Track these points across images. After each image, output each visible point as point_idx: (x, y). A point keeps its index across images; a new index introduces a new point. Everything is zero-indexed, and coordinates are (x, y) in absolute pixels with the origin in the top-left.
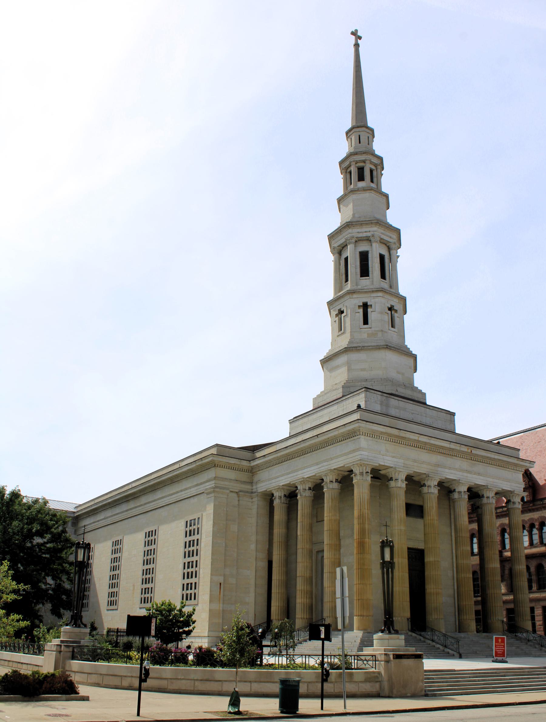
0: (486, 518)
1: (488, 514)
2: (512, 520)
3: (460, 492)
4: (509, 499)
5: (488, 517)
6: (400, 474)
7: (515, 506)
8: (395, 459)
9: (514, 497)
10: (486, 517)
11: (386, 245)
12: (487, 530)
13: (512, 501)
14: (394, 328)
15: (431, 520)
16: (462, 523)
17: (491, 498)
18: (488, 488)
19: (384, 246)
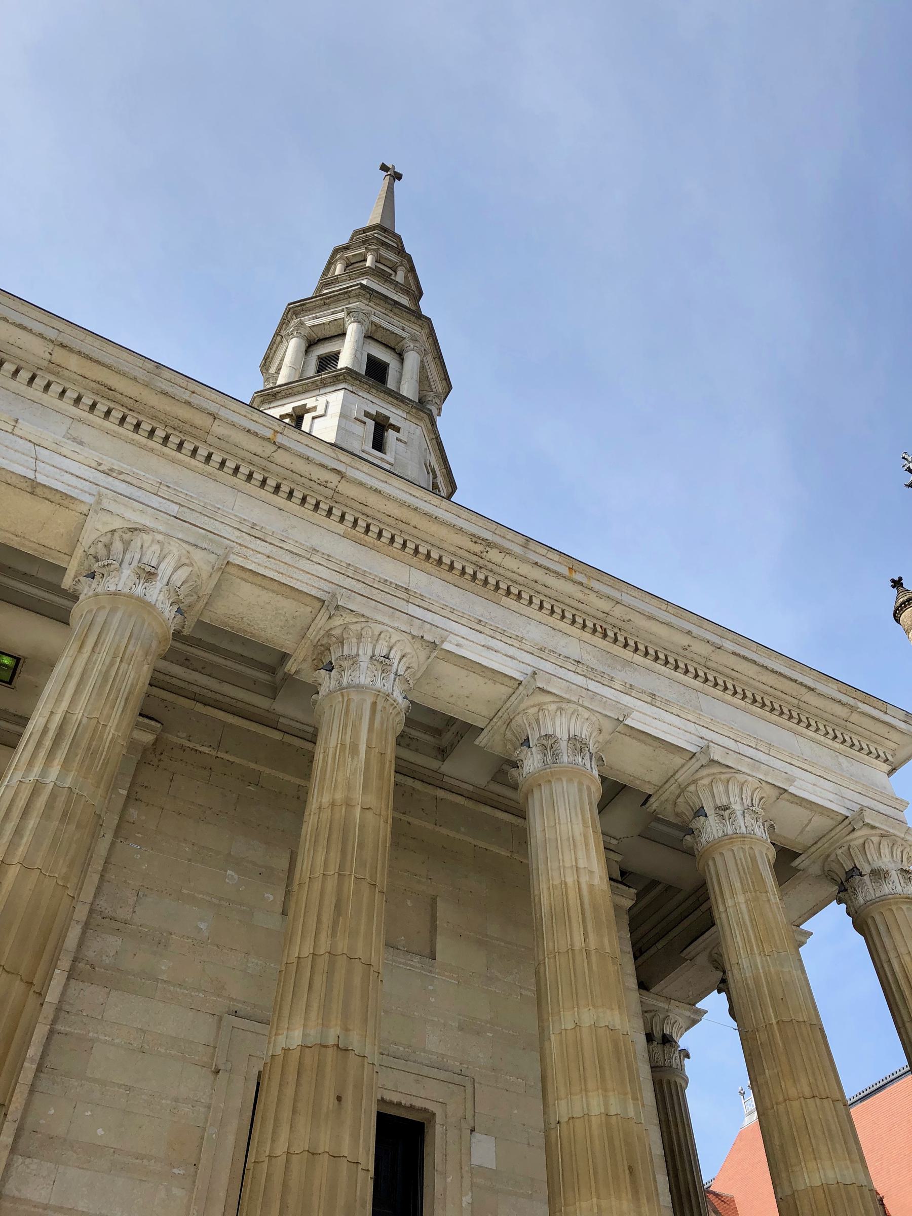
0: (731, 911)
1: (738, 885)
2: (892, 955)
3: (549, 745)
4: (848, 866)
5: (741, 899)
6: (137, 543)
7: (887, 889)
8: (117, 482)
9: (871, 851)
10: (730, 903)
11: (393, 349)
12: (745, 962)
13: (866, 869)
14: (385, 454)
15: (333, 804)
16: (570, 880)
17: (739, 813)
18: (713, 761)
19: (389, 351)
